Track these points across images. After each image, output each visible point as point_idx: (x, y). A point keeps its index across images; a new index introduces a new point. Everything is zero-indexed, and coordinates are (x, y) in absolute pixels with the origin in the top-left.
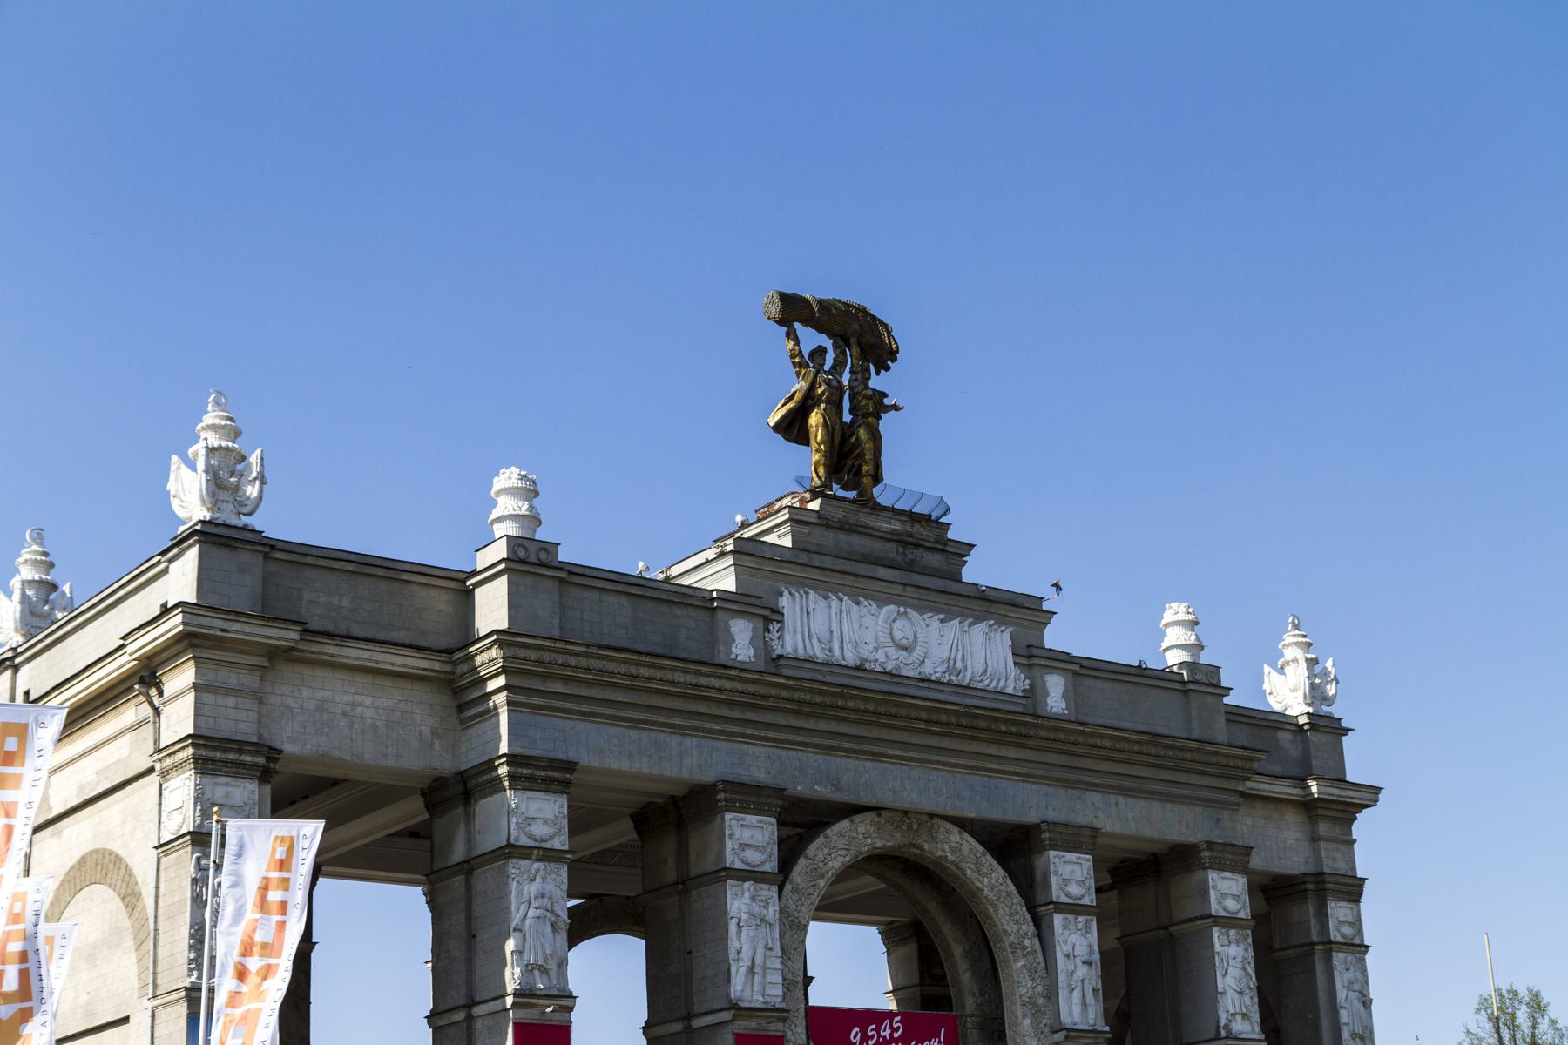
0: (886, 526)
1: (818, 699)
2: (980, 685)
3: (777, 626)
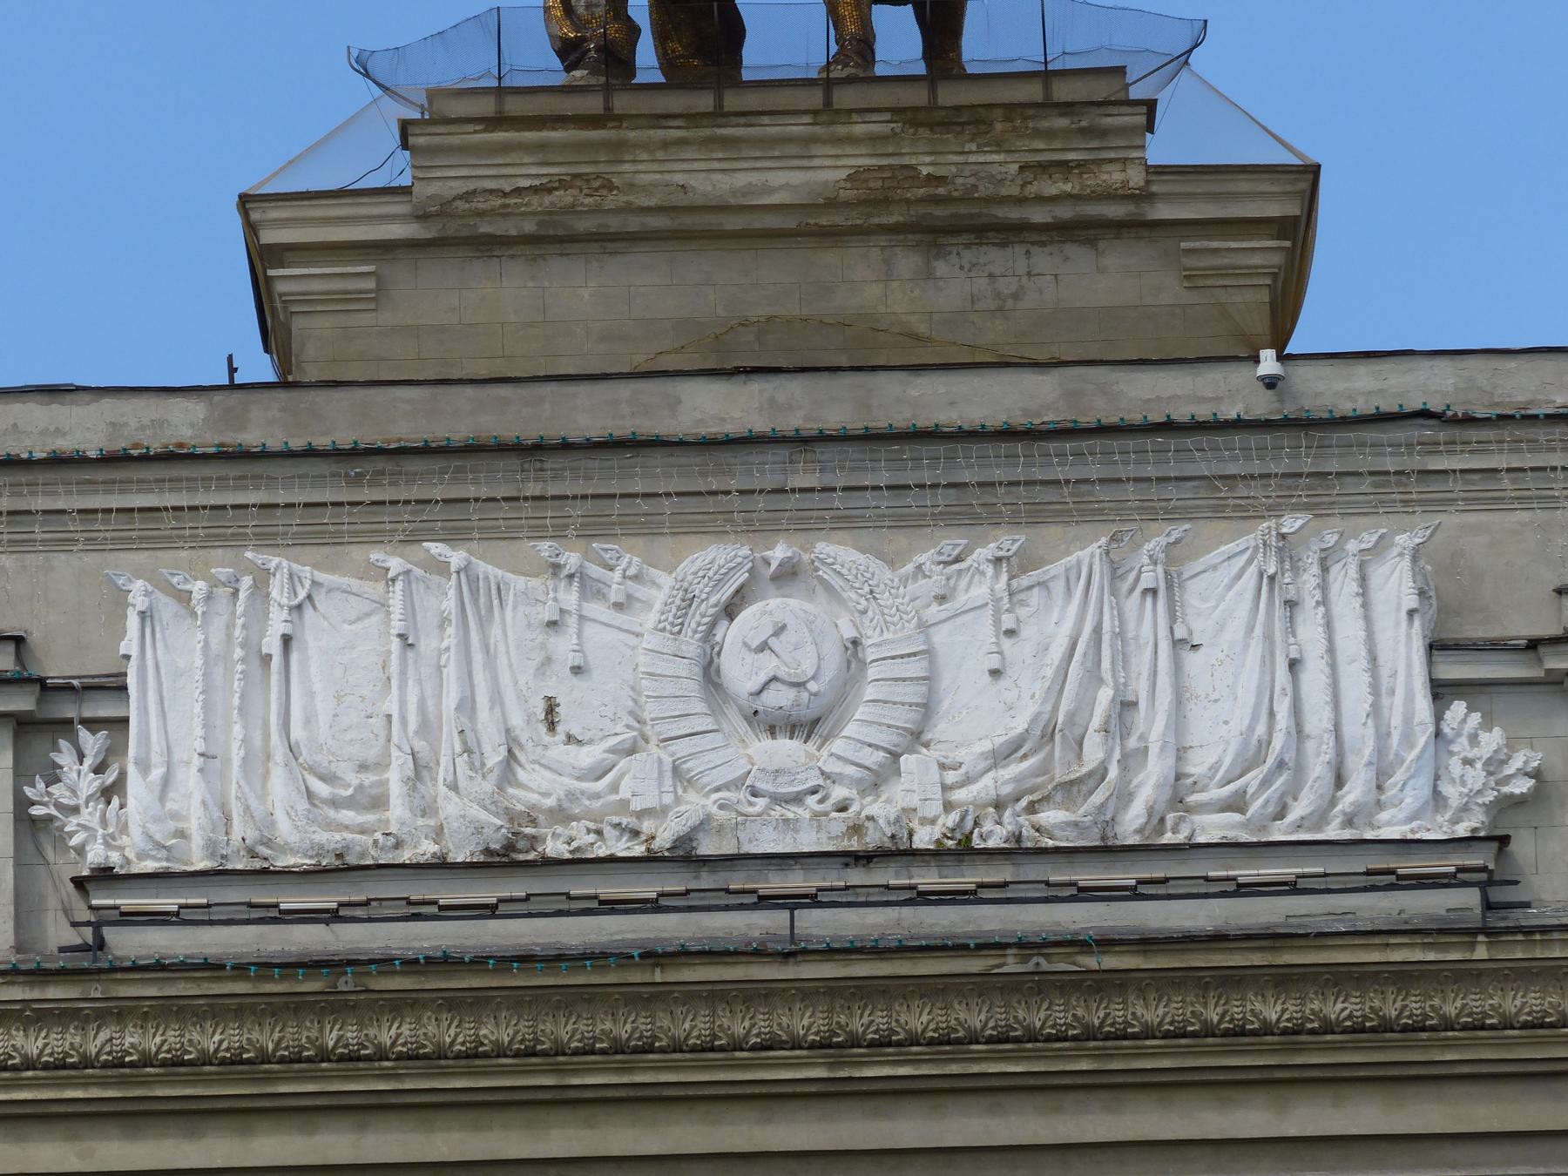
0: (784, 182)
1: (214, 1039)
2: (1212, 827)
3: (92, 742)
